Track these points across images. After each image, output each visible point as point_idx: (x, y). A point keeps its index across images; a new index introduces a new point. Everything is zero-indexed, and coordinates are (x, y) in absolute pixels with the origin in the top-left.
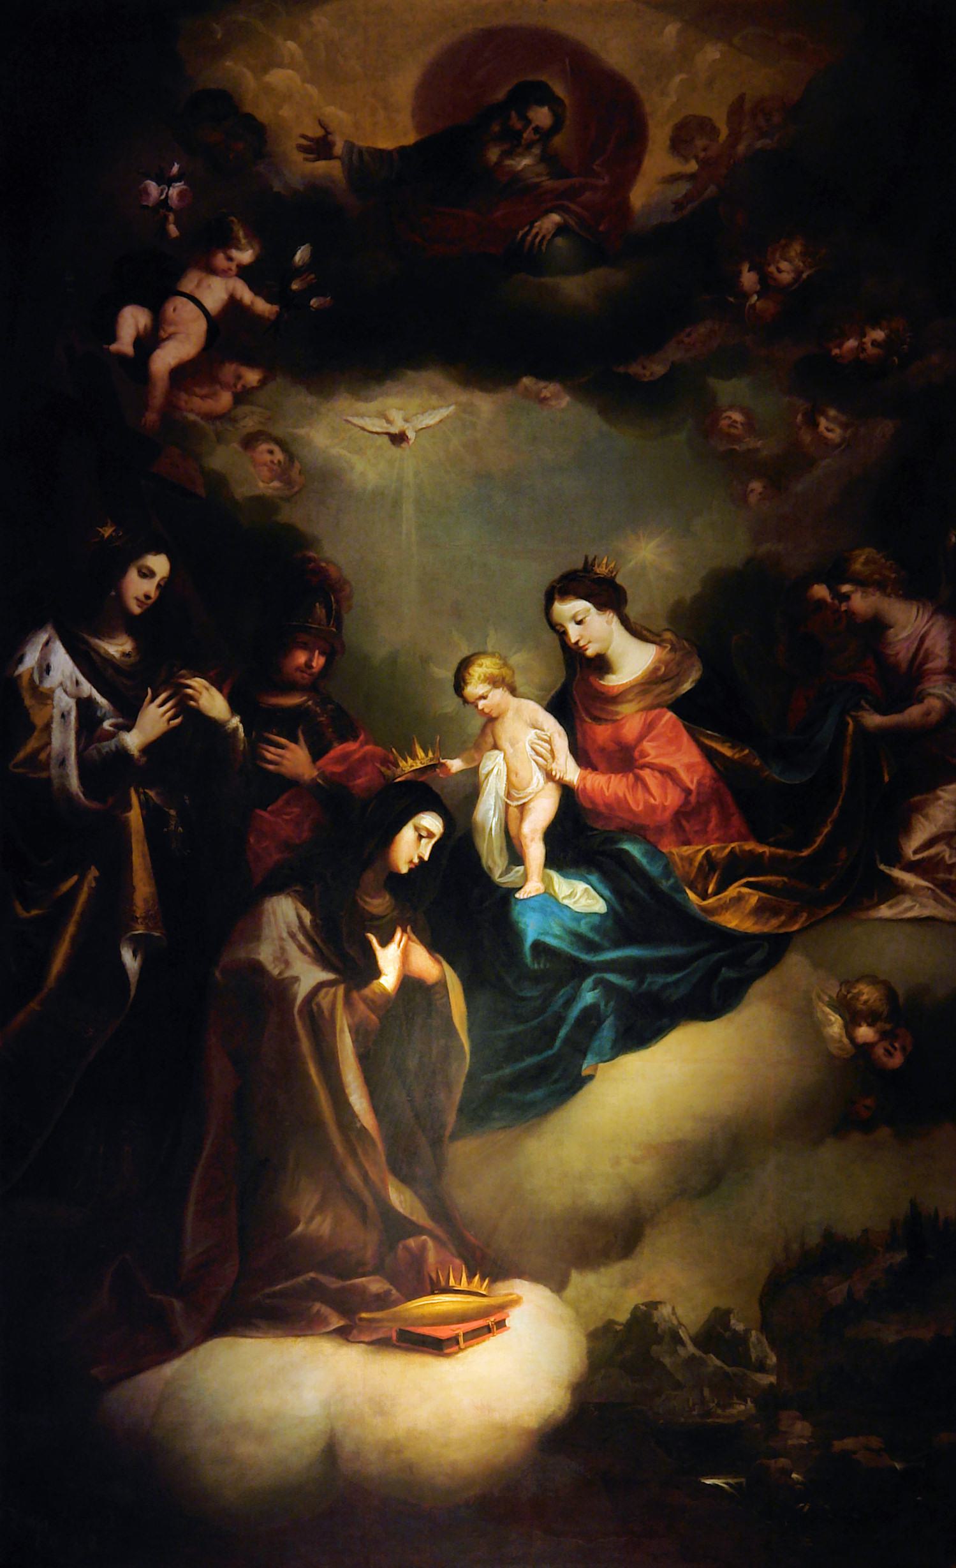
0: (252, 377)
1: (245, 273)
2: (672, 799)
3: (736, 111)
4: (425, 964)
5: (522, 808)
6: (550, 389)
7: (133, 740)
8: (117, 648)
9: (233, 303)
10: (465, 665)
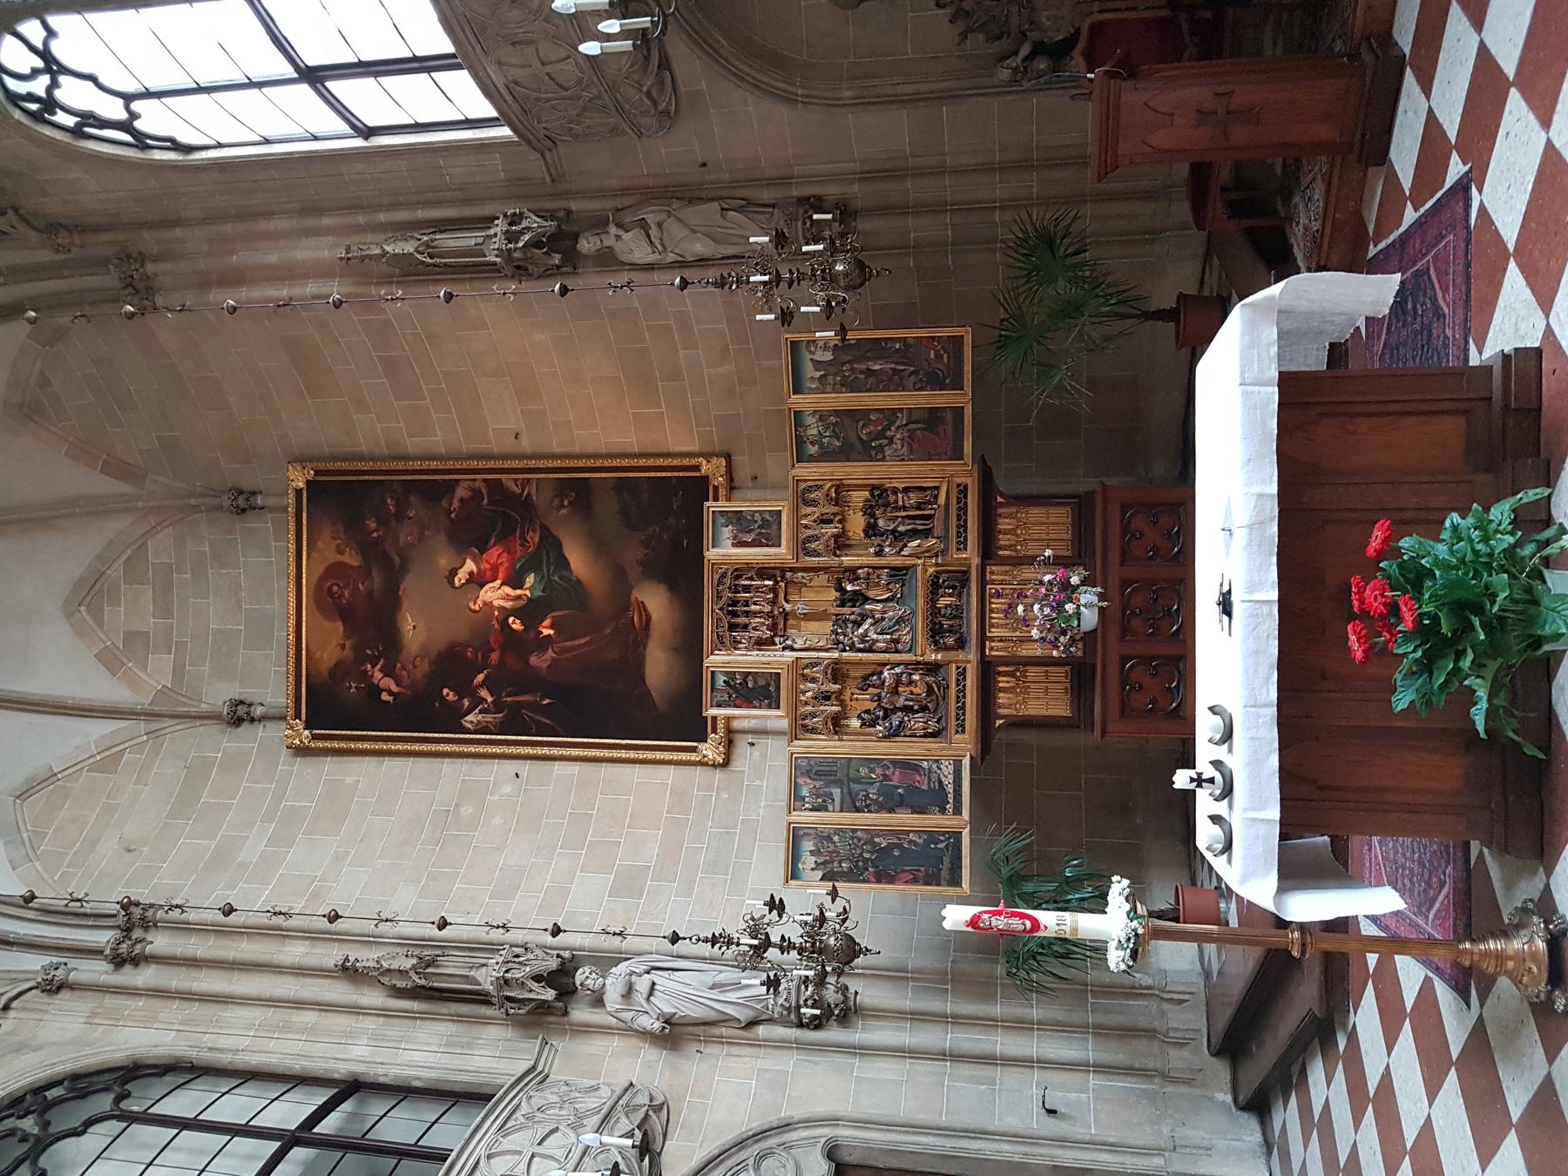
0: (399, 665)
1: (373, 667)
2: (505, 555)
3: (334, 538)
4: (547, 622)
5: (508, 595)
6: (402, 587)
7: (490, 699)
8: (466, 703)
9: (380, 670)
10: (470, 610)
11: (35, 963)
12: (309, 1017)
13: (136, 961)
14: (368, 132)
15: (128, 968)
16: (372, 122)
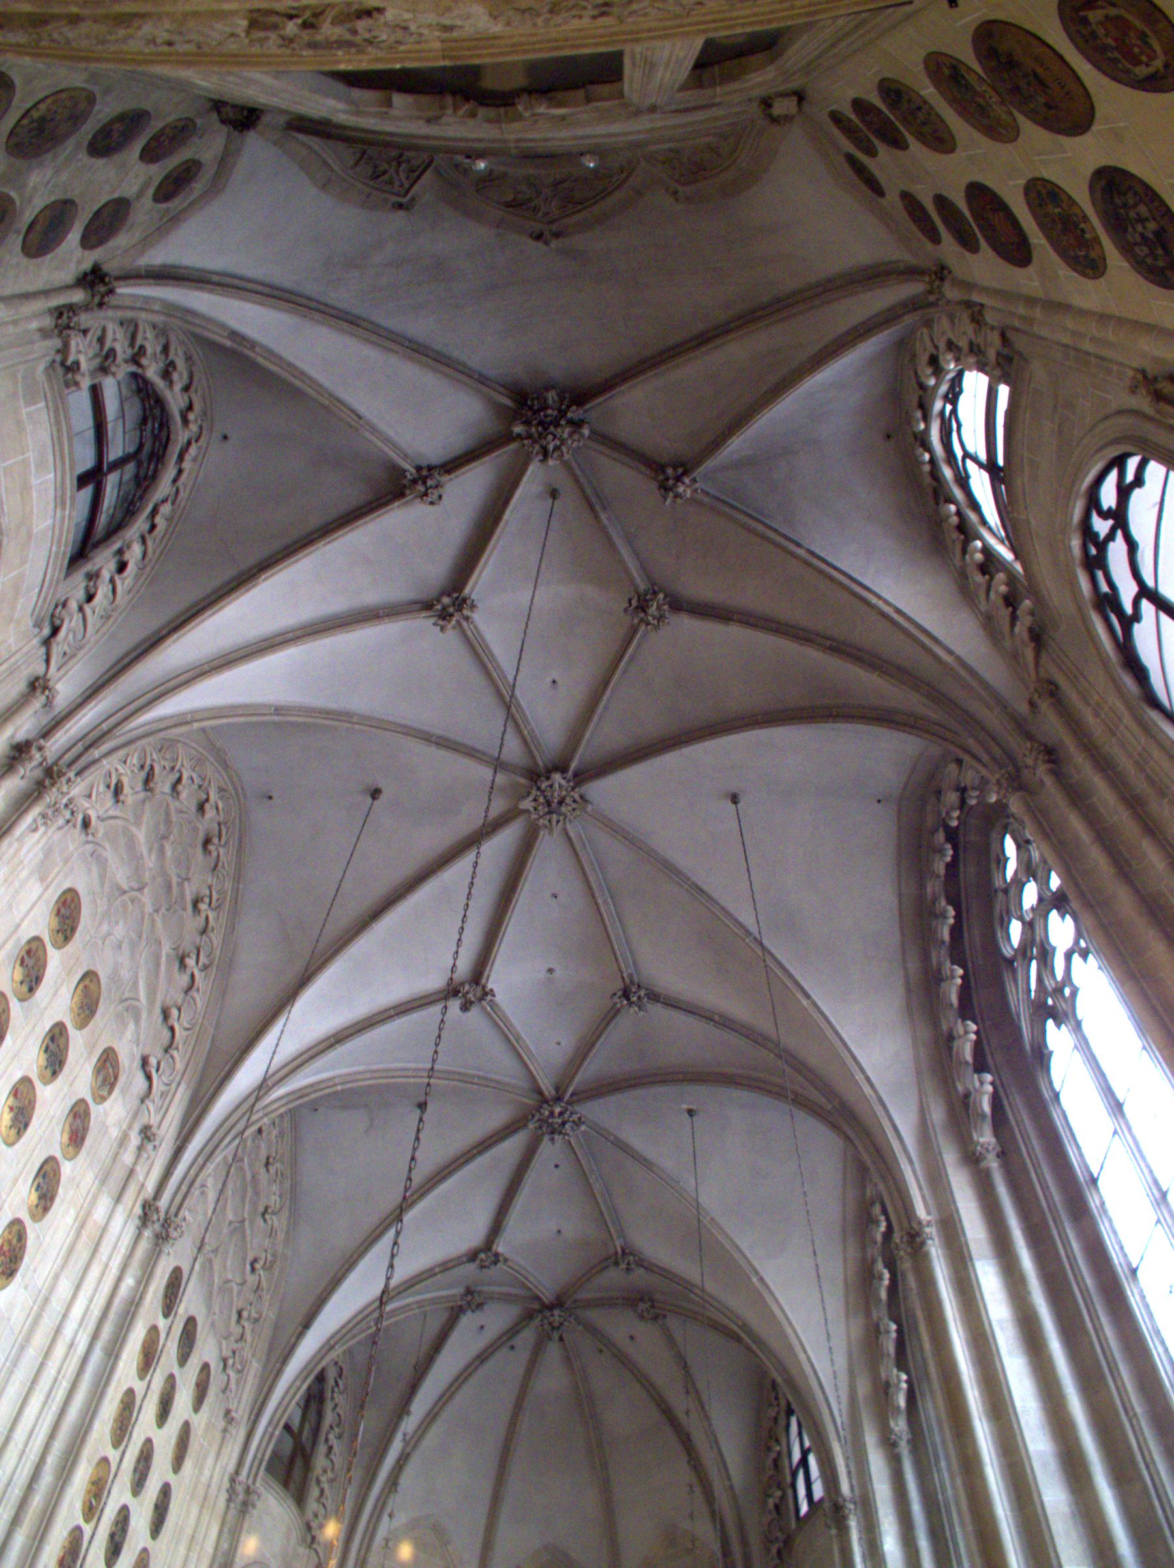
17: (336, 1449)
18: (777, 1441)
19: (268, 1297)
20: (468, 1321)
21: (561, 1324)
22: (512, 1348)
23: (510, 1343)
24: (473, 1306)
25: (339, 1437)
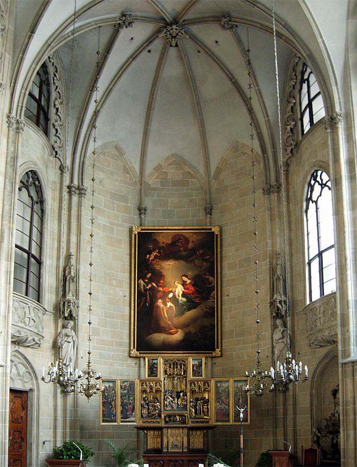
11: (68, 163)
12: (56, 245)
13: (70, 192)
14: (309, 264)
15: (67, 190)
16: (312, 264)
17: (60, 109)
18: (294, 97)
19: (7, 16)
20: (124, 33)
21: (177, 34)
22: (149, 51)
23: (148, 48)
24: (127, 23)
25: (61, 103)
